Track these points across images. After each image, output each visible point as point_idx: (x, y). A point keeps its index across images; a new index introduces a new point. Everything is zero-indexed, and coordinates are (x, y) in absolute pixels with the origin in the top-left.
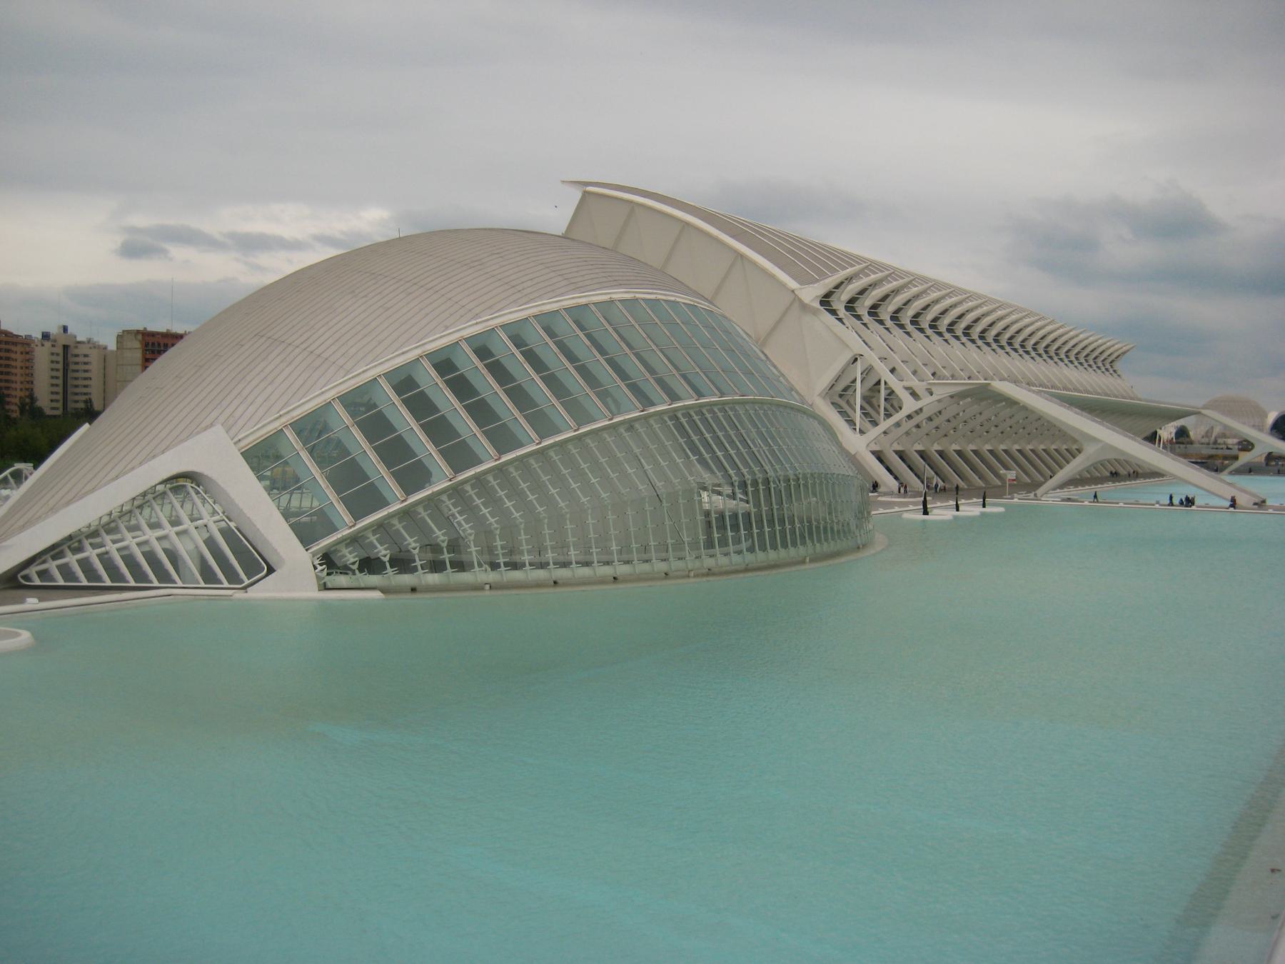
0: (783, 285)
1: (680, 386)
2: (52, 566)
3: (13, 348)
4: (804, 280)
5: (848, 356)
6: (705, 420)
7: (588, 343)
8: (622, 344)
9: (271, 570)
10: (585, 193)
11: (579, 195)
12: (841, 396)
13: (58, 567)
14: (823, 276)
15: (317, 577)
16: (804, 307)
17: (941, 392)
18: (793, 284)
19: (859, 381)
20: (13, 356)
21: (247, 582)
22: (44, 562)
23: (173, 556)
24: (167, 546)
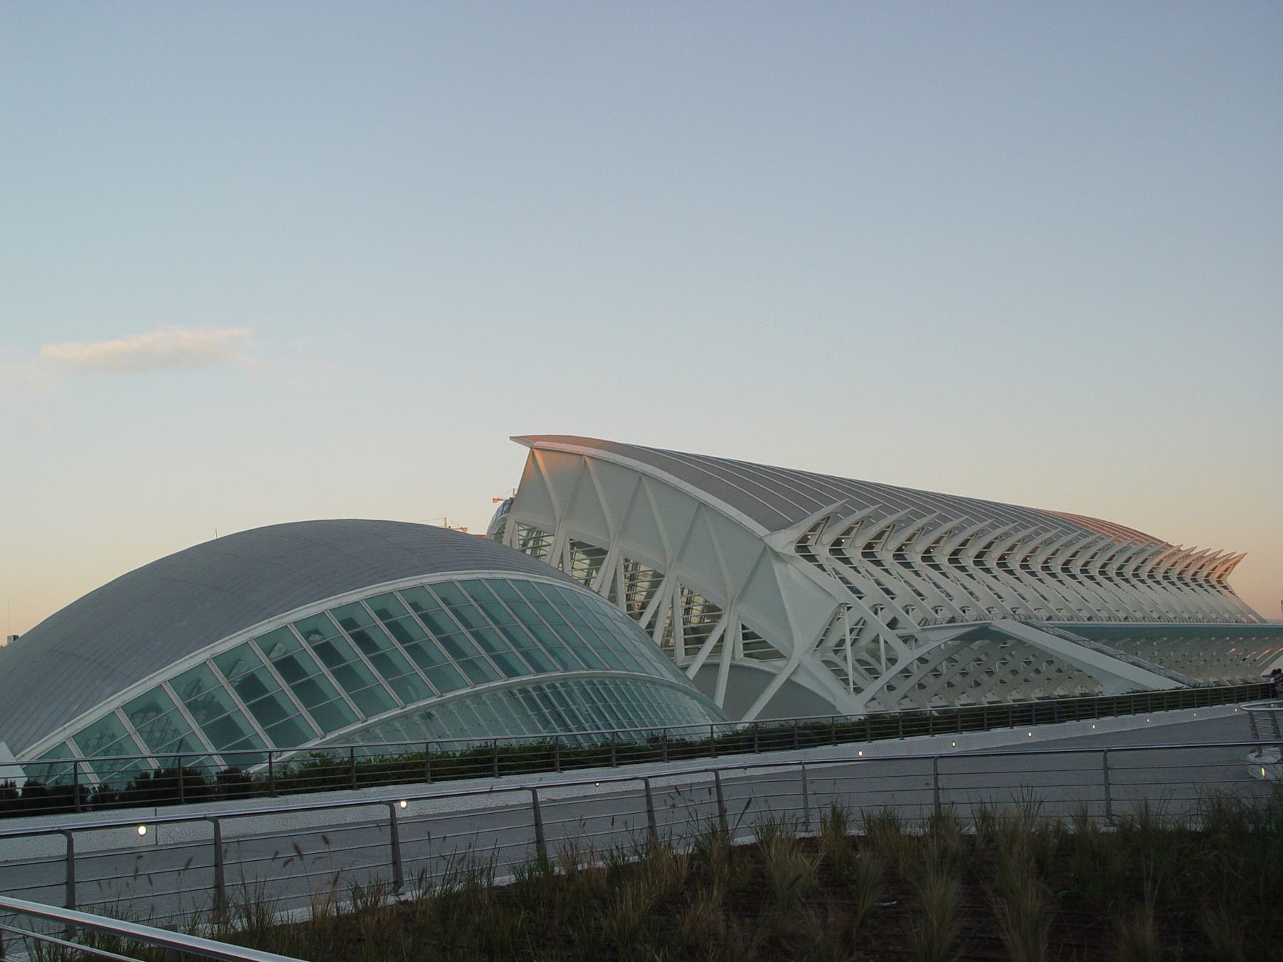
0: (751, 533)
4: (775, 525)
5: (832, 607)
6: (545, 697)
8: (488, 619)
11: (526, 451)
12: (836, 652)
14: (800, 517)
16: (777, 555)
17: (939, 639)
18: (760, 530)
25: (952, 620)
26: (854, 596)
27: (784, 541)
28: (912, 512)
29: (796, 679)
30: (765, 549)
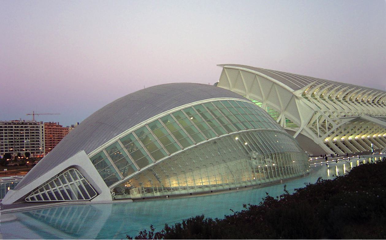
1: (231, 126)
2: (34, 196)
3: (63, 130)
4: (296, 89)
5: (313, 112)
7: (201, 116)
9: (98, 194)
10: (224, 68)
11: (221, 69)
13: (36, 196)
15: (112, 196)
16: (297, 97)
18: (292, 90)
19: (317, 121)
20: (63, 133)
21: (91, 198)
22: (32, 195)
23: (69, 191)
24: (67, 188)
25: (345, 116)
26: (319, 109)
27: (298, 93)
28: (334, 85)
29: (302, 133)
30: (293, 96)
